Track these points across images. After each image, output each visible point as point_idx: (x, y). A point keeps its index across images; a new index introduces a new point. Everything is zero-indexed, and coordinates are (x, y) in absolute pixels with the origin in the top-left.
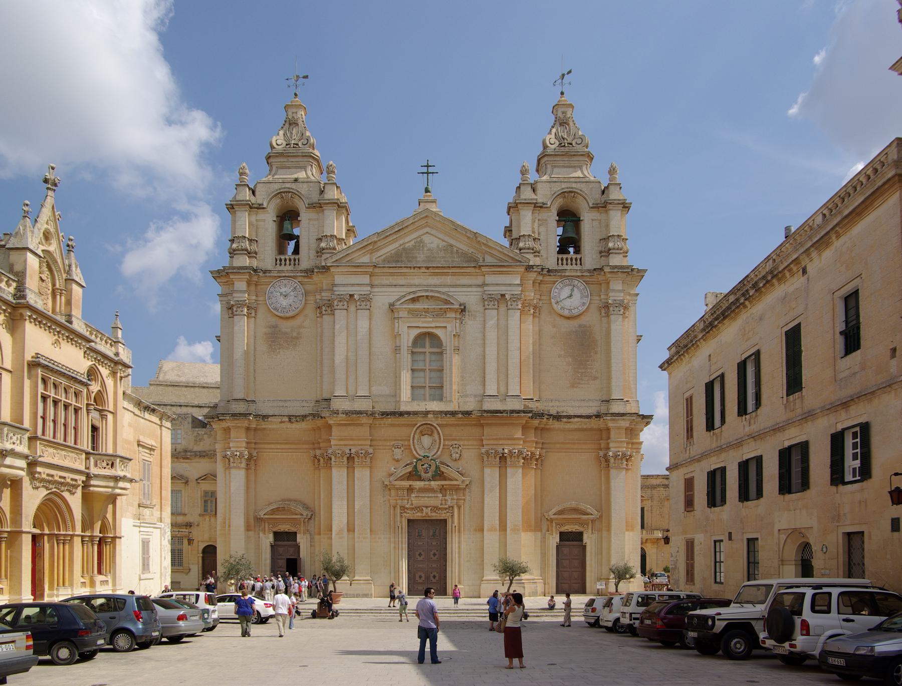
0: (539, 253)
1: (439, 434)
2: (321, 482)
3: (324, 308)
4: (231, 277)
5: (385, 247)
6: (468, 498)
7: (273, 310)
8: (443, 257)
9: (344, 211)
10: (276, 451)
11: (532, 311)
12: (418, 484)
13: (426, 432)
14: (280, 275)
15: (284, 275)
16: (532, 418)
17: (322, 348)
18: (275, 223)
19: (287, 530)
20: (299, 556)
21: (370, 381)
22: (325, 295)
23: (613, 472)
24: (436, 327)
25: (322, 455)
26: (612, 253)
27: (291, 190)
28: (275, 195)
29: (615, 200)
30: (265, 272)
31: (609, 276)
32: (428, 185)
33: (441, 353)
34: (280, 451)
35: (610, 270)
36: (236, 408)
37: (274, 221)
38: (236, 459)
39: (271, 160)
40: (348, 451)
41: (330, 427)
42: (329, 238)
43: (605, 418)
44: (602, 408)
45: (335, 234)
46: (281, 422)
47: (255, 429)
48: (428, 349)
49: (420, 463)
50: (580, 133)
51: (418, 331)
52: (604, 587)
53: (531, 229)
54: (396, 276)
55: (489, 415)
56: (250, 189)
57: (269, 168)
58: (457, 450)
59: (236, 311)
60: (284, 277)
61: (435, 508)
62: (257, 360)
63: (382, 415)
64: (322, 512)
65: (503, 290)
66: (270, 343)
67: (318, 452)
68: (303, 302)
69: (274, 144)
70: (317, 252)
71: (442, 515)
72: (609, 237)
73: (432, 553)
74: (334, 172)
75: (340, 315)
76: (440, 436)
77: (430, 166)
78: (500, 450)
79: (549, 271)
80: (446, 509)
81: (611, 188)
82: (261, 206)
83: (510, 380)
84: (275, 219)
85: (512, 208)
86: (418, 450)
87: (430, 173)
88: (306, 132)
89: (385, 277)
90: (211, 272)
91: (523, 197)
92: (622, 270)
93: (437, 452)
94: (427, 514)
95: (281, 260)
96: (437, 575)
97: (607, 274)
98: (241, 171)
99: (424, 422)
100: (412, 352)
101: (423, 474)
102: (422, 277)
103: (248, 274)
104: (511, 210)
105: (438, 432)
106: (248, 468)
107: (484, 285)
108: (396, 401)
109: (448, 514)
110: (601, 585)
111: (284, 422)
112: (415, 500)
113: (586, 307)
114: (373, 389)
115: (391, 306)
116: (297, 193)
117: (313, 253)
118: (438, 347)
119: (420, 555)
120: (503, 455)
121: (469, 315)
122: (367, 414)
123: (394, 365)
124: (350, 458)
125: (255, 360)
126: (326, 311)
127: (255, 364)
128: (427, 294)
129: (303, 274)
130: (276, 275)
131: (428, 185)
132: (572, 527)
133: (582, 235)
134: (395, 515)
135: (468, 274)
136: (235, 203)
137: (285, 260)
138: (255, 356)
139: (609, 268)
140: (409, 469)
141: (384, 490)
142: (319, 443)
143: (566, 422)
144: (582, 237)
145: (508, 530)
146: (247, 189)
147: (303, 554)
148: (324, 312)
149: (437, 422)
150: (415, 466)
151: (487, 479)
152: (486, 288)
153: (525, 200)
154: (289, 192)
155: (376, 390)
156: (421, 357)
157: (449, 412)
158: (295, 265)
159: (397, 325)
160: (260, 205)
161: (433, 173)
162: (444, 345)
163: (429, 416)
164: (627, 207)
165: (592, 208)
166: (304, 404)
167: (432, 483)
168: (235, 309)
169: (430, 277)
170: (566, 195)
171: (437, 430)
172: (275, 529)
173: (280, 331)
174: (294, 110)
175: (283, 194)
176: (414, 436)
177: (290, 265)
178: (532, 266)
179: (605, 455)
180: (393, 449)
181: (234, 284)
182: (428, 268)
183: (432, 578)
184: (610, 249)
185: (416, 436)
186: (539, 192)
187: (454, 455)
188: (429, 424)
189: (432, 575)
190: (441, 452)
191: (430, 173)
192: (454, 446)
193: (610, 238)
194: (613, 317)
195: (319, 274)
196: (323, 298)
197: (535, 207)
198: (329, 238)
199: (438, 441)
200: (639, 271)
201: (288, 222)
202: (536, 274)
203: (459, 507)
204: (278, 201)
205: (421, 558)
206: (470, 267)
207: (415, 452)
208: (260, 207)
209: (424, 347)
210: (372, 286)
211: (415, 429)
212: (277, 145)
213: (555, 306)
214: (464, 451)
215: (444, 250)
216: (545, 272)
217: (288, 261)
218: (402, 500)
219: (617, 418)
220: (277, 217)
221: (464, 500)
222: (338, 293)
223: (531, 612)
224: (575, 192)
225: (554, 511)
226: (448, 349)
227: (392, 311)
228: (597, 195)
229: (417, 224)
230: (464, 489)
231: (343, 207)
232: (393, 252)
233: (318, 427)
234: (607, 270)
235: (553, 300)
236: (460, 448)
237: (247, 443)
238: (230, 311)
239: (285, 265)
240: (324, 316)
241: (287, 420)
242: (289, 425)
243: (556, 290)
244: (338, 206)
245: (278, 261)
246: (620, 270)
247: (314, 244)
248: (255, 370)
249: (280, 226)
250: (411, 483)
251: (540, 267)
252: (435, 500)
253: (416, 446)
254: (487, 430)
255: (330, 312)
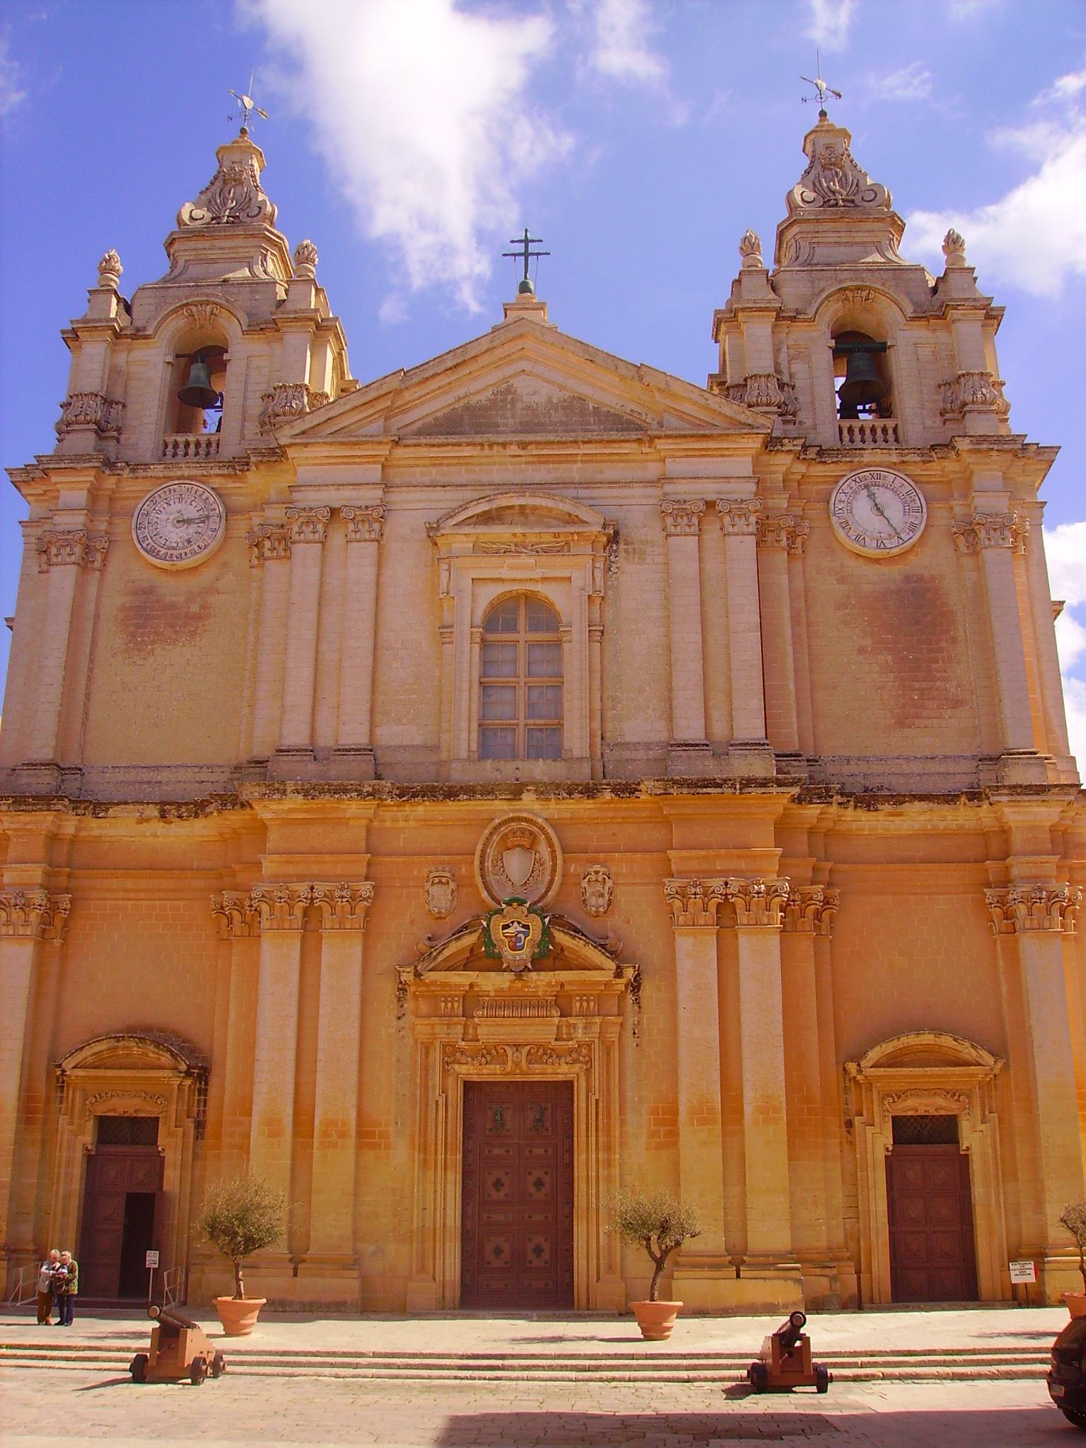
0: (794, 414)
1: (551, 845)
2: (233, 977)
3: (267, 544)
4: (54, 479)
5: (423, 403)
6: (631, 1020)
7: (142, 551)
8: (562, 423)
9: (332, 339)
10: (121, 895)
11: (784, 543)
12: (491, 982)
13: (516, 841)
14: (171, 474)
15: (179, 473)
16: (798, 800)
17: (257, 638)
18: (170, 368)
19: (131, 1113)
20: (162, 1187)
21: (372, 712)
22: (276, 514)
23: (1029, 945)
24: (545, 579)
25: (239, 906)
26: (970, 412)
27: (213, 299)
28: (175, 311)
29: (966, 300)
30: (134, 467)
31: (968, 460)
32: (526, 278)
33: (558, 644)
34: (132, 895)
35: (971, 447)
36: (29, 785)
37: (168, 363)
38: (14, 916)
39: (176, 246)
40: (302, 888)
41: (261, 828)
42: (290, 392)
43: (996, 798)
44: (982, 775)
45: (307, 382)
46: (142, 820)
47: (74, 840)
48: (523, 635)
49: (498, 922)
50: (869, 181)
51: (499, 589)
52: (1031, 1279)
53: (771, 363)
54: (448, 465)
55: (685, 791)
56: (119, 300)
57: (168, 263)
58: (599, 887)
59: (57, 556)
60: (179, 478)
61: (541, 1052)
62: (96, 671)
63: (401, 796)
64: (230, 1063)
65: (710, 490)
66: (132, 629)
67: (228, 896)
68: (220, 532)
69: (186, 217)
70: (263, 424)
71: (562, 1071)
72: (959, 377)
73: (531, 1179)
74: (313, 261)
75: (306, 553)
76: (553, 852)
77: (533, 241)
78: (717, 883)
79: (821, 453)
80: (570, 1051)
81: (955, 279)
82: (141, 333)
83: (736, 704)
84: (170, 359)
85: (726, 321)
86: (495, 888)
87: (533, 254)
88: (257, 195)
89: (419, 469)
90: (10, 472)
91: (746, 296)
92: (1000, 448)
93: (547, 892)
94: (517, 1064)
95: (176, 445)
96: (546, 1246)
97: (965, 455)
98: (104, 264)
99: (511, 815)
100: (483, 641)
101: (508, 953)
102: (510, 467)
103: (93, 472)
104: (723, 328)
105: (549, 840)
106: (43, 938)
107: (663, 479)
108: (441, 763)
109: (577, 1066)
110: (1023, 1273)
111: (148, 820)
112: (488, 1030)
113: (919, 534)
114: (378, 731)
115: (433, 532)
116: (225, 303)
117: (252, 429)
118: (548, 630)
119: (498, 1184)
120: (726, 899)
121: (626, 551)
122: (360, 793)
123: (437, 673)
124: (311, 912)
125: (91, 670)
126: (273, 549)
127: (89, 678)
128: (522, 501)
129: (226, 472)
130: (161, 475)
131: (526, 278)
132: (925, 1101)
133: (895, 375)
134: (426, 1068)
135: (623, 458)
136: (80, 325)
137: (187, 445)
138: (91, 661)
139: (967, 440)
140: (469, 940)
141: (399, 999)
142: (234, 875)
143: (891, 815)
144: (895, 383)
145: (748, 1110)
146: (114, 300)
147: (172, 1179)
148: (268, 554)
149: (545, 814)
150: (486, 931)
151: (685, 965)
152: (668, 488)
153: (755, 302)
154: (207, 303)
155: (388, 735)
156: (508, 654)
157: (578, 785)
158: (208, 454)
159: (445, 576)
160: (138, 330)
161: (538, 254)
162: (565, 620)
163: (525, 796)
164: (995, 318)
165: (912, 319)
166: (205, 775)
167: (534, 975)
168: (54, 551)
169: (530, 467)
170: (850, 294)
171: (546, 834)
172: (103, 1109)
173: (158, 601)
174: (237, 158)
175: (194, 309)
176: (483, 852)
177: (197, 454)
178: (779, 440)
179: (1002, 901)
180: (428, 885)
181: (57, 498)
182: (523, 445)
183: (531, 1256)
184: (965, 404)
185: (491, 852)
186: (785, 290)
187: (593, 901)
188: (526, 820)
189: (530, 1246)
190: (558, 894)
191: (533, 254)
192: (593, 877)
193: (962, 380)
194: (989, 555)
195: (261, 467)
196: (269, 521)
197: (778, 318)
198: (290, 392)
199: (549, 864)
200: (1040, 450)
201: (200, 364)
202: (792, 456)
203: (608, 1050)
204: (178, 323)
205: (501, 1195)
206: (628, 441)
207: (485, 894)
208: (138, 334)
209: (513, 628)
210: (387, 486)
211: (487, 832)
212: (192, 218)
213: (841, 534)
214: (618, 890)
215: (563, 408)
216: (812, 454)
217: (192, 447)
218: (449, 1025)
219: (1026, 798)
220: (177, 356)
221: (622, 1025)
222: (302, 505)
223: (835, 1365)
224: (870, 288)
225: (874, 1055)
226: (575, 629)
227: (436, 544)
228: (923, 297)
229: (499, 352)
230: (622, 997)
231: (328, 329)
232: (439, 414)
233: (235, 831)
234: (963, 445)
235: (834, 519)
236: (609, 883)
237: (48, 874)
238: (44, 557)
239: (186, 454)
240: (267, 563)
241: (156, 813)
242: (159, 827)
243: (842, 497)
244: (318, 327)
245: (170, 450)
246: (996, 447)
247: (256, 407)
248: (88, 696)
249: (184, 375)
250: (472, 976)
251: (800, 442)
252: (542, 1030)
253: (491, 878)
254: (678, 834)
255: (283, 554)
